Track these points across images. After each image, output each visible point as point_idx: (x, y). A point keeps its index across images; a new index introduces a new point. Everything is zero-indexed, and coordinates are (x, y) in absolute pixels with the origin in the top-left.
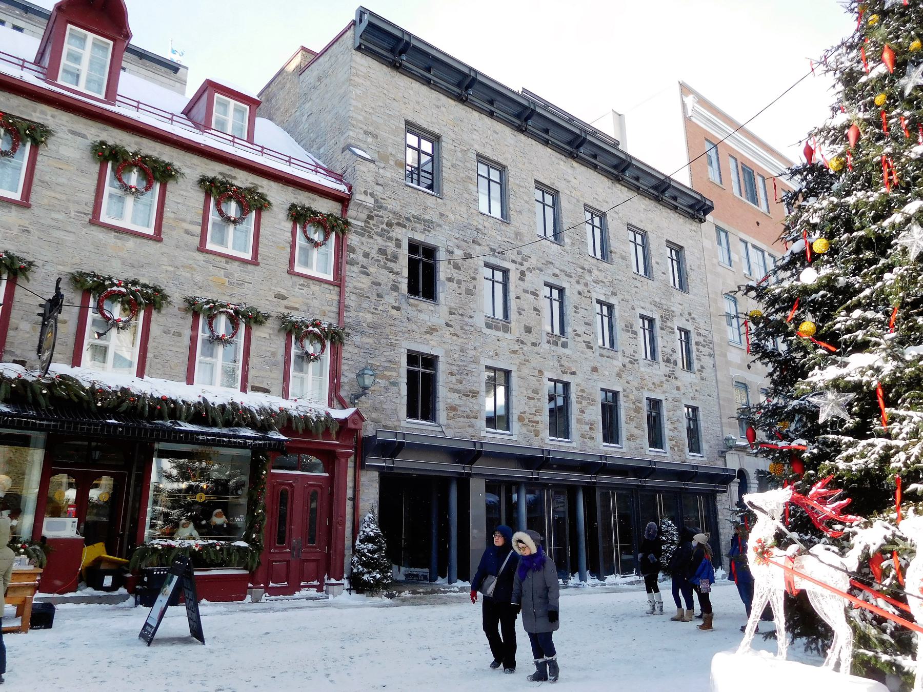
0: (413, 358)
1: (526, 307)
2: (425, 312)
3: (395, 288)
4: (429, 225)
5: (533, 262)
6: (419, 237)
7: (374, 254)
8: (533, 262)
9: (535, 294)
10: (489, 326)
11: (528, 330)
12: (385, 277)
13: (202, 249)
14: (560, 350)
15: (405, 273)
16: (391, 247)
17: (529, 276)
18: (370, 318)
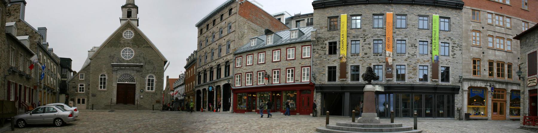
0: (330, 68)
1: (365, 48)
2: (333, 57)
3: (325, 54)
4: (334, 38)
5: (370, 35)
6: (331, 41)
7: (320, 48)
8: (370, 35)
9: (369, 44)
10: (352, 56)
11: (366, 54)
12: (322, 52)
13: (287, 60)
14: (379, 57)
15: (328, 50)
16: (324, 46)
17: (367, 40)
18: (319, 62)
